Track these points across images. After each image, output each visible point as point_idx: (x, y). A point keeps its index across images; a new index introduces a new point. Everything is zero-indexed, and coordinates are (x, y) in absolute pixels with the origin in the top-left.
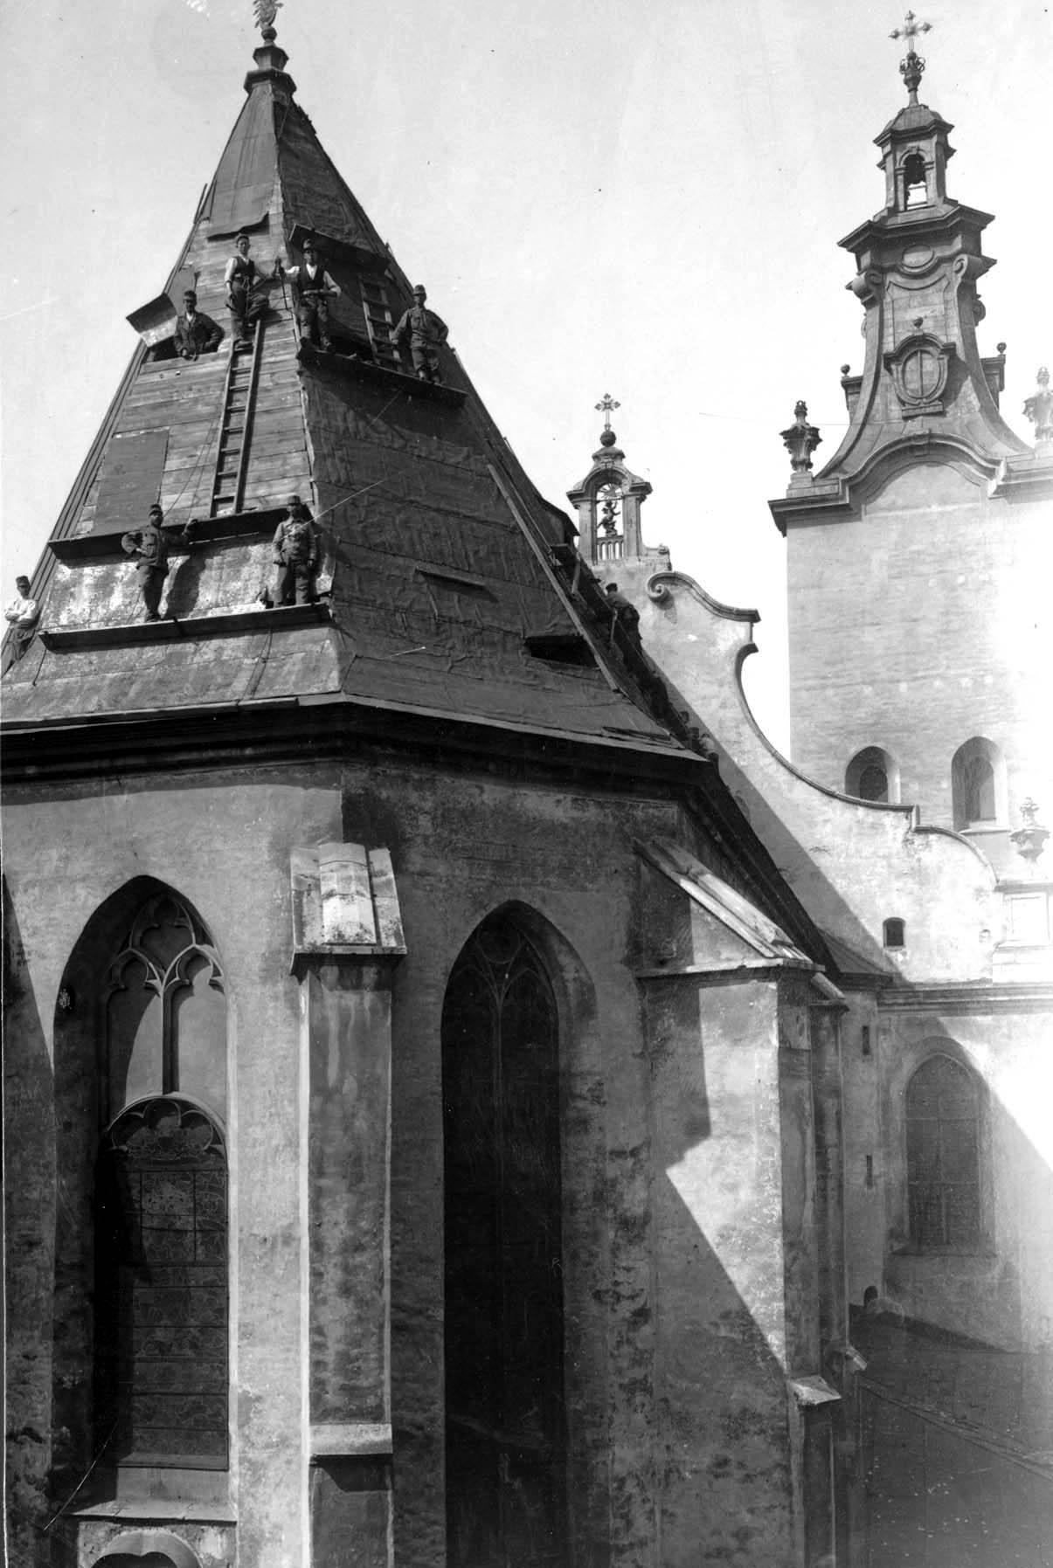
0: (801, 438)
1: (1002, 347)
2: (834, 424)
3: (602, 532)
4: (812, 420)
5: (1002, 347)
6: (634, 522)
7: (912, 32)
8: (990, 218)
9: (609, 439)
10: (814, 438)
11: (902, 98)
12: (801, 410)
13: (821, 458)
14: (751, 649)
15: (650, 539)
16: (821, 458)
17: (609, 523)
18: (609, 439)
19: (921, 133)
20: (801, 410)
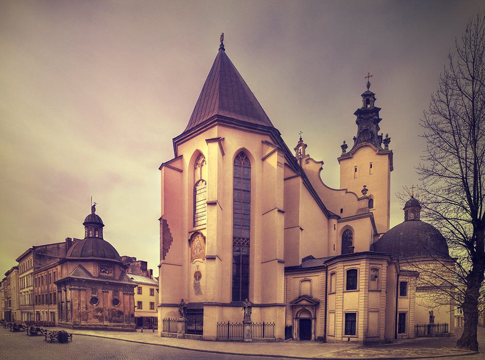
3: (299, 154)
6: (304, 152)
14: (321, 169)
17: (300, 153)
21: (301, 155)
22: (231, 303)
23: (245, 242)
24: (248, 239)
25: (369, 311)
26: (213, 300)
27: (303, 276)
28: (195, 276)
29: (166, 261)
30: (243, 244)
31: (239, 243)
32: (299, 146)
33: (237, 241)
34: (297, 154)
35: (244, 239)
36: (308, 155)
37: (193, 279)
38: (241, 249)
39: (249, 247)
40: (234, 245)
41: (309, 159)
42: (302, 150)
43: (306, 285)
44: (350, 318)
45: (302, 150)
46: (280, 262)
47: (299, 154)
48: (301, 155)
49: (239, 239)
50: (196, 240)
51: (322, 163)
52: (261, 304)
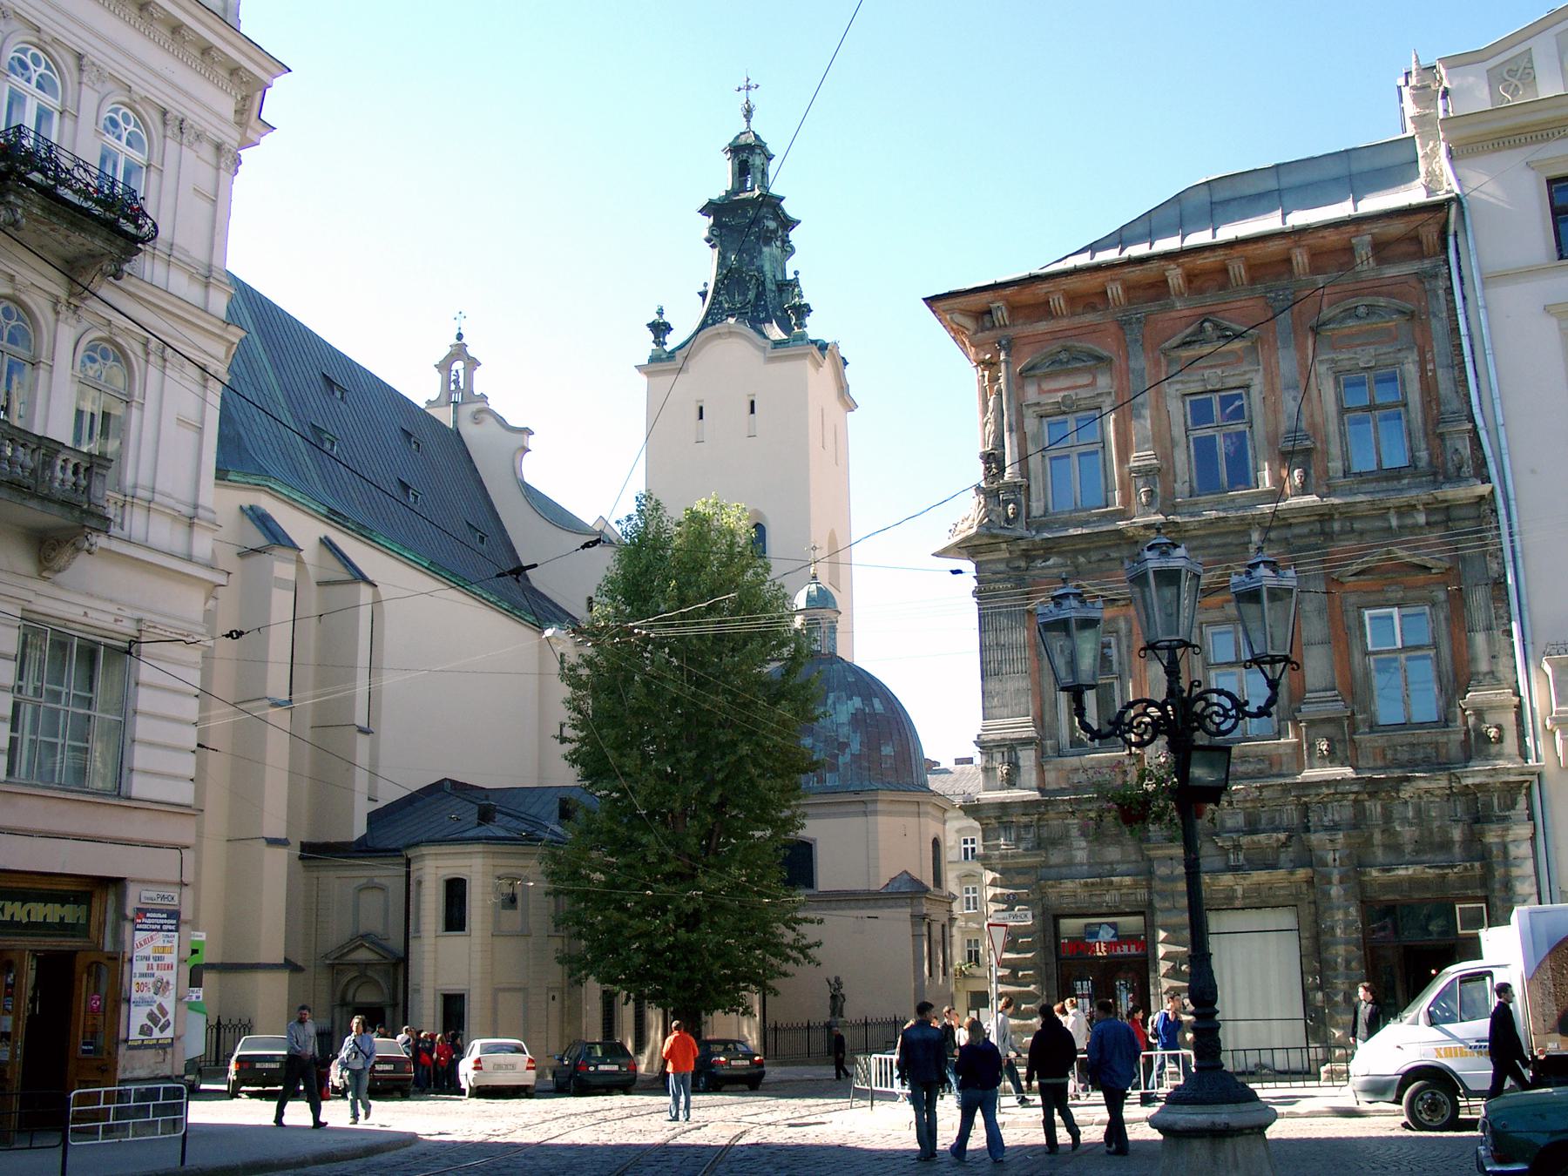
0: (660, 329)
1: (796, 273)
2: (686, 317)
3: (453, 387)
4: (666, 318)
5: (796, 273)
7: (749, 88)
8: (782, 199)
9: (460, 336)
10: (667, 328)
11: (743, 128)
12: (660, 313)
13: (672, 341)
15: (477, 392)
16: (672, 341)
17: (457, 382)
18: (460, 336)
19: (749, 148)
20: (660, 313)
34: (446, 382)
36: (483, 397)
41: (483, 412)
42: (461, 373)
43: (371, 900)
45: (461, 373)
46: (273, 842)
47: (453, 387)
51: (527, 431)
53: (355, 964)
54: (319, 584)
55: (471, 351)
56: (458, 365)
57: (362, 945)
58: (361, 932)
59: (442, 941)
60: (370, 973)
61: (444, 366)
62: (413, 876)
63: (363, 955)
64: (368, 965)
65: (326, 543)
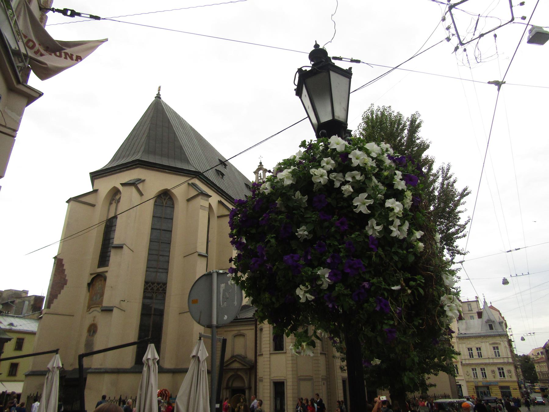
9: (261, 163)
17: (260, 177)
18: (261, 163)
21: (261, 179)
22: (132, 368)
23: (161, 287)
24: (165, 284)
25: (300, 379)
26: (101, 365)
27: (235, 329)
28: (89, 331)
29: (51, 310)
30: (158, 289)
31: (152, 289)
32: (259, 169)
33: (150, 286)
34: (257, 178)
35: (158, 284)
37: (85, 333)
38: (154, 296)
39: (165, 293)
40: (145, 290)
44: (279, 387)
45: (262, 174)
48: (261, 179)
49: (153, 283)
50: (97, 284)
52: (175, 369)
53: (233, 369)
54: (219, 217)
55: (264, 167)
56: (261, 172)
57: (235, 361)
58: (235, 354)
59: (274, 357)
60: (240, 373)
61: (256, 172)
62: (259, 327)
63: (236, 365)
64: (238, 369)
65: (220, 202)
